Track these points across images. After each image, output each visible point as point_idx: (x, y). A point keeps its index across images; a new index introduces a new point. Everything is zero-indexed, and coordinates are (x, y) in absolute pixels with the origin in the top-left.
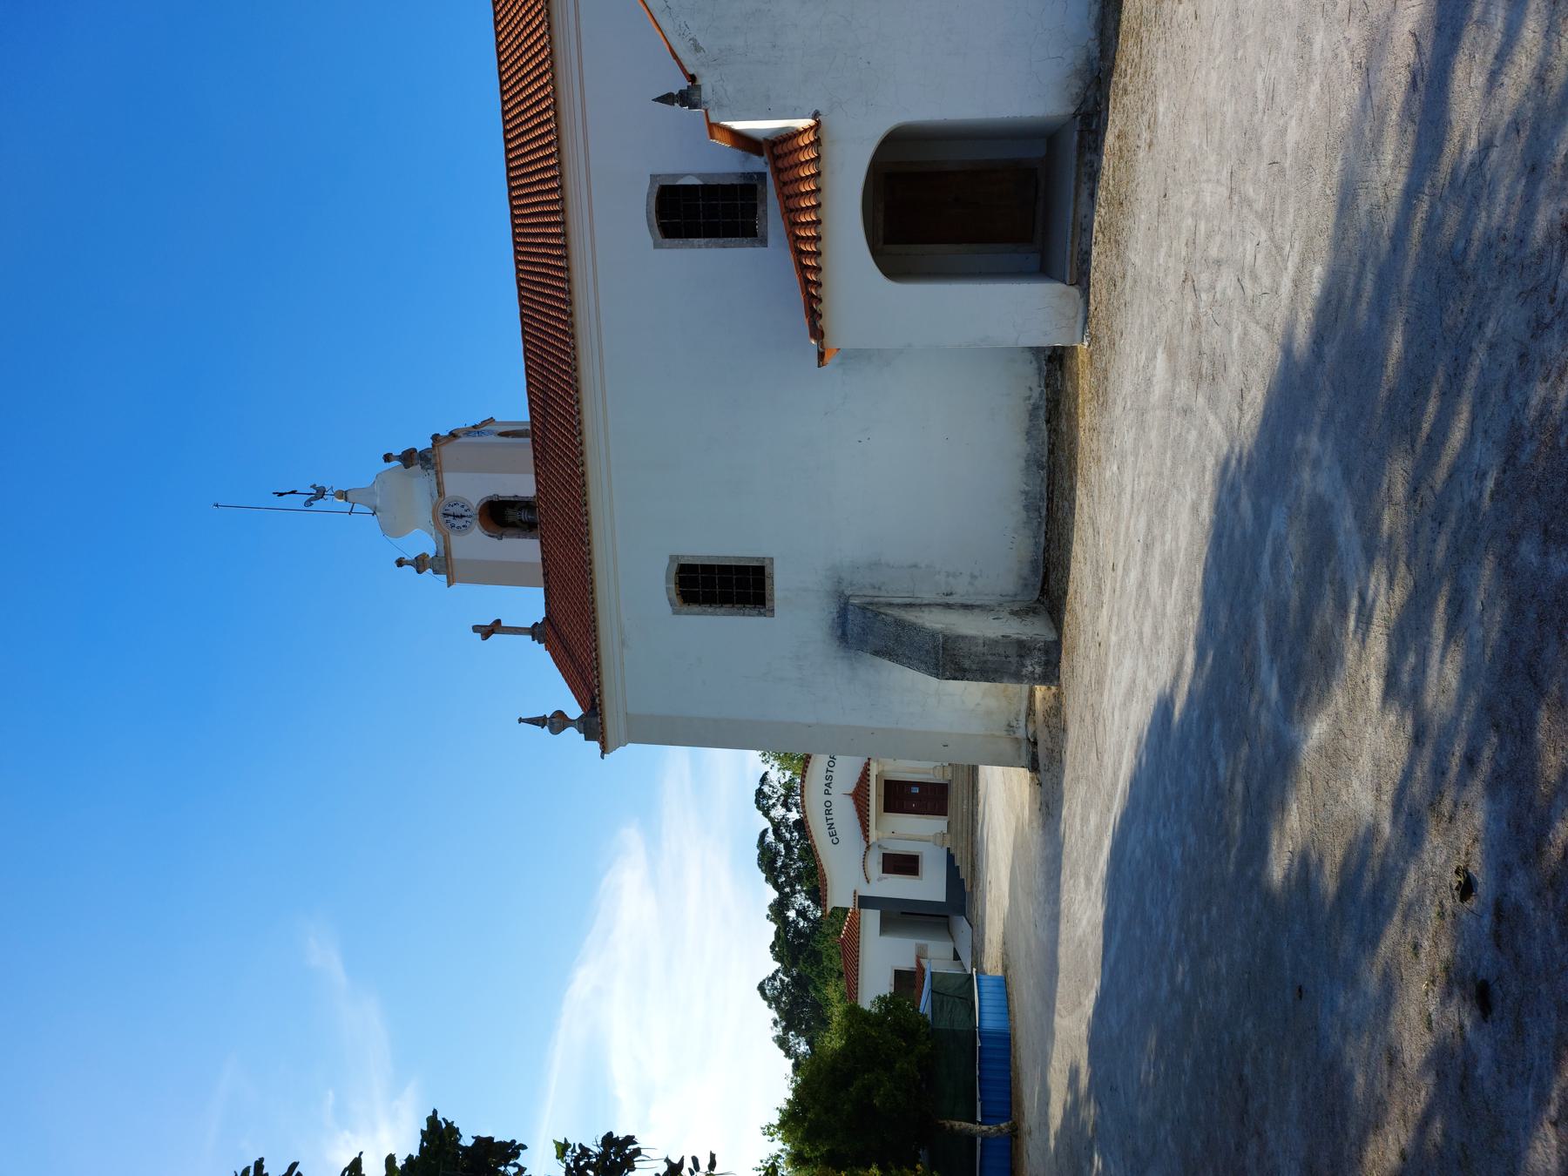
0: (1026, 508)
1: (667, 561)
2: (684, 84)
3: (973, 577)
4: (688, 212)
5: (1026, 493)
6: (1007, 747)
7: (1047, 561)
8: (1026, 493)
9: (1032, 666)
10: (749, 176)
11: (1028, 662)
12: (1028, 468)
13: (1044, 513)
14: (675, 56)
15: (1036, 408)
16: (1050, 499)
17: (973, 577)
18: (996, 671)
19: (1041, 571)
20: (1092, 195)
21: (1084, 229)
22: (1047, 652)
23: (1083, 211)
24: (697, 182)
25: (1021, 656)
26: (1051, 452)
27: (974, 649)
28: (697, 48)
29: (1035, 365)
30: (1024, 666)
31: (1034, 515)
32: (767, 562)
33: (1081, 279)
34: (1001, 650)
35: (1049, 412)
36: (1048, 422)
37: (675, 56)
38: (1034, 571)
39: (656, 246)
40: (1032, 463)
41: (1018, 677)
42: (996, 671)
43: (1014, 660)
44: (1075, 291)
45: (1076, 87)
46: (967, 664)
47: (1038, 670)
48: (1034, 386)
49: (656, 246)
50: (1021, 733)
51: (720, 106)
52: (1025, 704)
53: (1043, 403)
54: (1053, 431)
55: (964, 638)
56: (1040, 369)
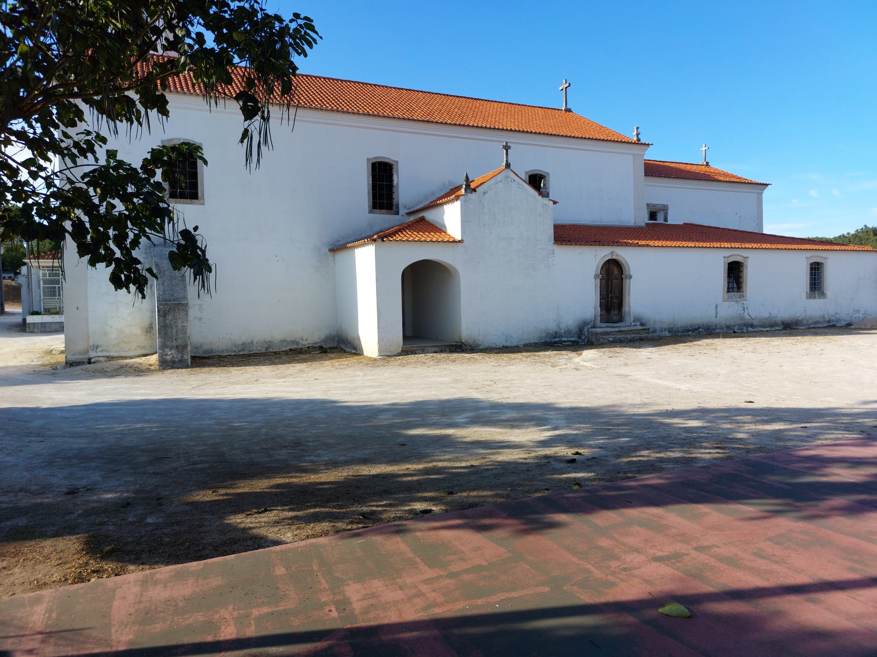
0: (244, 344)
1: (366, 161)
2: (473, 185)
3: (200, 319)
4: (382, 175)
5: (252, 343)
6: (81, 346)
7: (213, 357)
8: (252, 343)
9: (170, 354)
10: (398, 207)
11: (173, 351)
12: (266, 342)
13: (242, 353)
14: (482, 184)
15: (297, 343)
16: (250, 355)
17: (200, 319)
18: (166, 334)
19: (206, 355)
20: (436, 352)
21: (423, 351)
22: (181, 361)
23: (429, 349)
24: (395, 183)
25: (177, 347)
26: (275, 353)
27: (180, 321)
28: (484, 193)
29: (318, 341)
30: (171, 349)
31: (240, 348)
32: (201, 201)
33: (405, 352)
34: (180, 336)
35: (295, 350)
36: (290, 350)
37: (482, 184)
38: (206, 352)
39: (368, 159)
40: (269, 344)
41: (163, 346)
42: (166, 334)
43: (175, 343)
44: (400, 350)
45: (470, 342)
46: (169, 317)
47: (169, 358)
48: (308, 341)
49: (368, 159)
50: (92, 354)
51: (466, 201)
52: (115, 354)
53: (300, 347)
54: (286, 353)
55: (187, 315)
56: (317, 343)
